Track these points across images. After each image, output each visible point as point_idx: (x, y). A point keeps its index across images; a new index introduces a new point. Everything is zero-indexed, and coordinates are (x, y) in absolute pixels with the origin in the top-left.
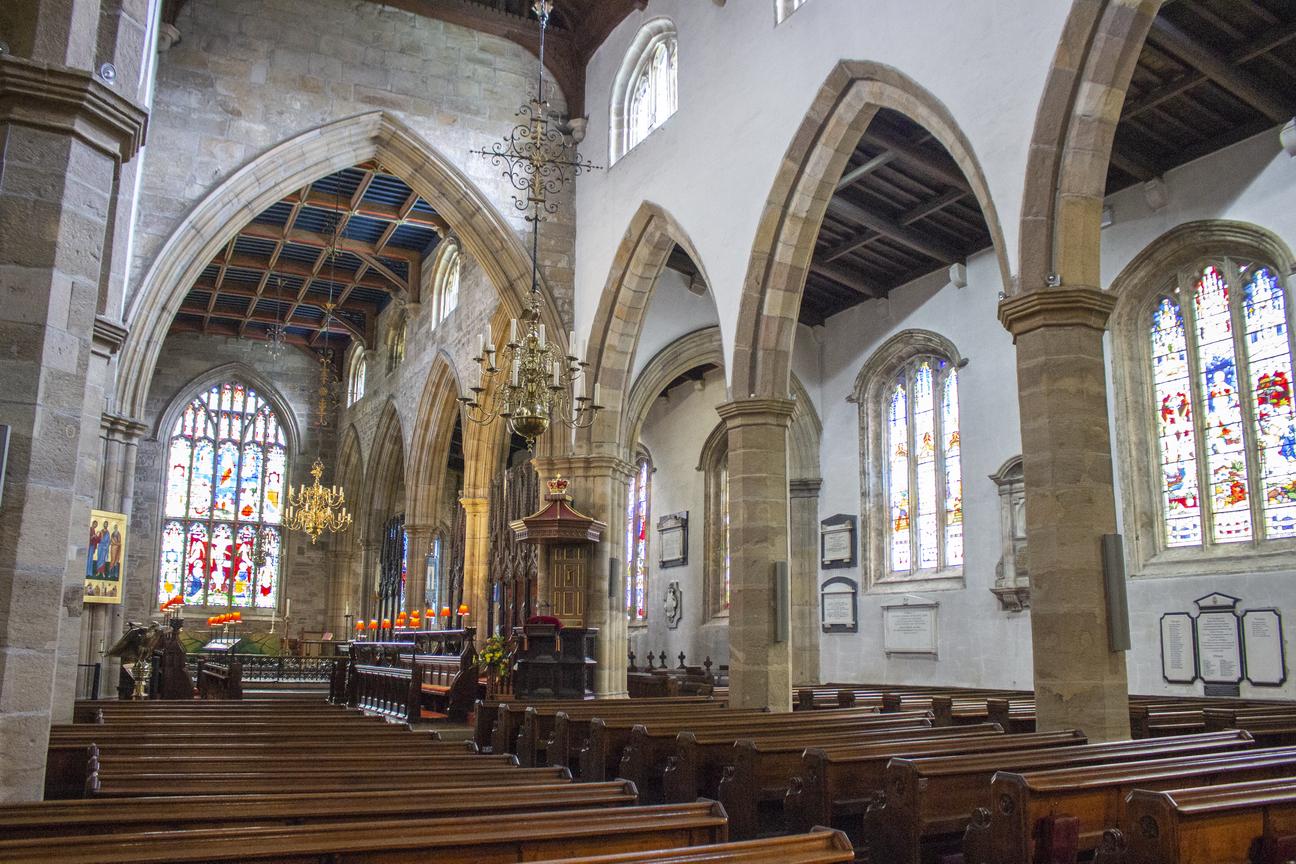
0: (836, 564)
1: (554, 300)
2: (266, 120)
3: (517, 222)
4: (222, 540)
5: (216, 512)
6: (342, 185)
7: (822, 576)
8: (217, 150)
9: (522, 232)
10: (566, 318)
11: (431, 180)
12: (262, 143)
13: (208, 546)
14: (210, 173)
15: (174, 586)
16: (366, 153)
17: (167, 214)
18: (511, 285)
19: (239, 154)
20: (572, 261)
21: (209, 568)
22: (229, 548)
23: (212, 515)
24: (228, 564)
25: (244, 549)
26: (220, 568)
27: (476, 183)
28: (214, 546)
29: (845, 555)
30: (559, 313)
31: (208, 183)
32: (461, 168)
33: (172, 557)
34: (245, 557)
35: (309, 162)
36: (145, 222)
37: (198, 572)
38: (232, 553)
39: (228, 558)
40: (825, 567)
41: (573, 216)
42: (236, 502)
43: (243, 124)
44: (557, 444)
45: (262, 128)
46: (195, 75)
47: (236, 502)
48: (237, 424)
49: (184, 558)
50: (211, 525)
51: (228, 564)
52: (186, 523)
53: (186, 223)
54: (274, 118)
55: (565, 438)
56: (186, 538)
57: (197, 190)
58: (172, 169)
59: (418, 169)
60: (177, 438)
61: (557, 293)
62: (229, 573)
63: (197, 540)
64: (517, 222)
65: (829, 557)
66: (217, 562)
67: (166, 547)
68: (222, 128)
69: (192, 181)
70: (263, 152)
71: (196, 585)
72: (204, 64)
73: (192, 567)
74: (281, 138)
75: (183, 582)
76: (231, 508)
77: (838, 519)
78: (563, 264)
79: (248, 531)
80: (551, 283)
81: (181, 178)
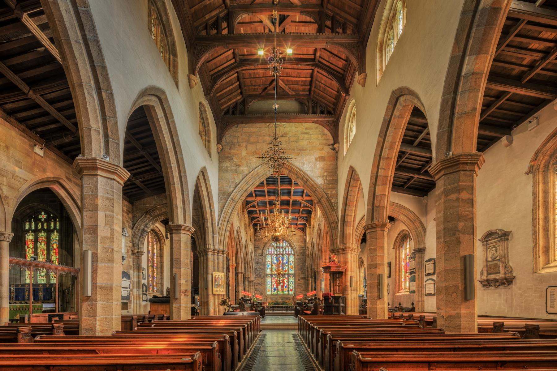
0: (429, 274)
2: (247, 166)
7: (425, 278)
8: (235, 177)
9: (321, 184)
10: (335, 208)
11: (294, 173)
12: (247, 173)
20: (337, 190)
27: (306, 172)
29: (432, 271)
32: (302, 168)
35: (260, 175)
40: (426, 275)
41: (337, 176)
43: (241, 168)
54: (249, 165)
58: (225, 185)
59: (290, 171)
61: (332, 201)
64: (320, 181)
65: (427, 272)
68: (236, 171)
69: (230, 187)
70: (247, 175)
77: (430, 260)
78: (334, 192)
81: (227, 186)
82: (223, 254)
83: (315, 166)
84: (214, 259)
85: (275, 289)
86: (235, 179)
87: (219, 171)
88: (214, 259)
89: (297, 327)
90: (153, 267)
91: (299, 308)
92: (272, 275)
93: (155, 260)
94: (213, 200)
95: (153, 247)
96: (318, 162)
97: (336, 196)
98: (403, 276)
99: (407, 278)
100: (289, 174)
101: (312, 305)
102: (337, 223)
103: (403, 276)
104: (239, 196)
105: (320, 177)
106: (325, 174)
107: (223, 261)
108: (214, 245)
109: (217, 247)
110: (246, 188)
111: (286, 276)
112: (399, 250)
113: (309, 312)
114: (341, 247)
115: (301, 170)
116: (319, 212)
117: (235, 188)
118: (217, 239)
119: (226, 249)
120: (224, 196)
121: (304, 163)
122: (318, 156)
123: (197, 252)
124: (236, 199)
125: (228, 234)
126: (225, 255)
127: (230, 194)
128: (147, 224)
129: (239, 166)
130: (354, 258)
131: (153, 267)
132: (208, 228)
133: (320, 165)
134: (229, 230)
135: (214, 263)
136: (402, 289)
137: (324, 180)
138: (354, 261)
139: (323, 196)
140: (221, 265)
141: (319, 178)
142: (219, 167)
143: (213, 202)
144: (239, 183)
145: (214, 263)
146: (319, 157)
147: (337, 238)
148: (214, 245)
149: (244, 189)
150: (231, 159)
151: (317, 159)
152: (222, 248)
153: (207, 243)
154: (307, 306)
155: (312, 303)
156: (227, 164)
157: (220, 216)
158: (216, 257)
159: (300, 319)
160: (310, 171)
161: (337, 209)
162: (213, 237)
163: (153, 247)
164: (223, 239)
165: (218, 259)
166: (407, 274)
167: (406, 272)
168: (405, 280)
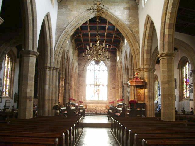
1: (135, 37)
2: (77, 11)
3: (127, 22)
6: (92, 21)
9: (128, 24)
10: (138, 40)
14: (67, 23)
16: (96, 13)
17: (60, 31)
18: (127, 35)
19: (72, 18)
20: (138, 28)
27: (117, 16)
30: (136, 39)
31: (67, 24)
32: (114, 14)
36: (57, 32)
41: (138, 20)
43: (73, 13)
44: (137, 66)
45: (76, 13)
46: (64, 6)
53: (64, 32)
55: (139, 64)
57: (65, 26)
61: (136, 36)
64: (127, 22)
69: (64, 24)
71: (93, 96)
72: (66, 3)
74: (80, 14)
78: (137, 29)
80: (134, 34)
82: (57, 70)
83: (123, 13)
84: (50, 74)
85: (93, 96)
86: (68, 19)
87: (58, 14)
88: (50, 74)
89: (111, 126)
90: (7, 78)
91: (111, 111)
92: (90, 85)
93: (9, 73)
94: (52, 33)
95: (8, 64)
96: (125, 11)
97: (138, 32)
98: (185, 88)
99: (188, 90)
100: (105, 17)
101: (121, 109)
102: (139, 51)
103: (185, 88)
104: (71, 31)
105: (126, 19)
106: (130, 18)
107: (56, 75)
108: (50, 64)
109: (53, 65)
110: (76, 25)
111: (101, 86)
112: (182, 70)
113: (118, 114)
114: (142, 67)
115: (114, 15)
116: (126, 41)
117: (68, 25)
118: (53, 60)
119: (59, 67)
120: (60, 30)
121: (116, 11)
122: (125, 7)
123: (38, 68)
124: (68, 33)
125: (61, 56)
126: (58, 71)
127: (64, 29)
128: (6, 49)
129: (72, 11)
130: (151, 75)
131: (7, 78)
132: (47, 52)
133: (126, 12)
134: (62, 53)
135: (50, 77)
136: (184, 98)
137: (129, 22)
138: (151, 78)
139: (129, 32)
140: (54, 78)
141: (126, 21)
142: (58, 12)
143: (52, 34)
144: (71, 22)
145: (50, 77)
146: (126, 7)
147: (139, 61)
148: (50, 64)
149: (74, 26)
150: (66, 7)
151: (124, 9)
152: (56, 66)
153: (46, 62)
154: (117, 109)
155: (120, 107)
156: (64, 10)
157: (56, 43)
158: (51, 72)
159: (112, 120)
160: (120, 15)
161: (139, 41)
162: (50, 58)
163: (8, 64)
164: (57, 60)
165: (53, 73)
166: (188, 87)
167: (187, 86)
168: (186, 91)
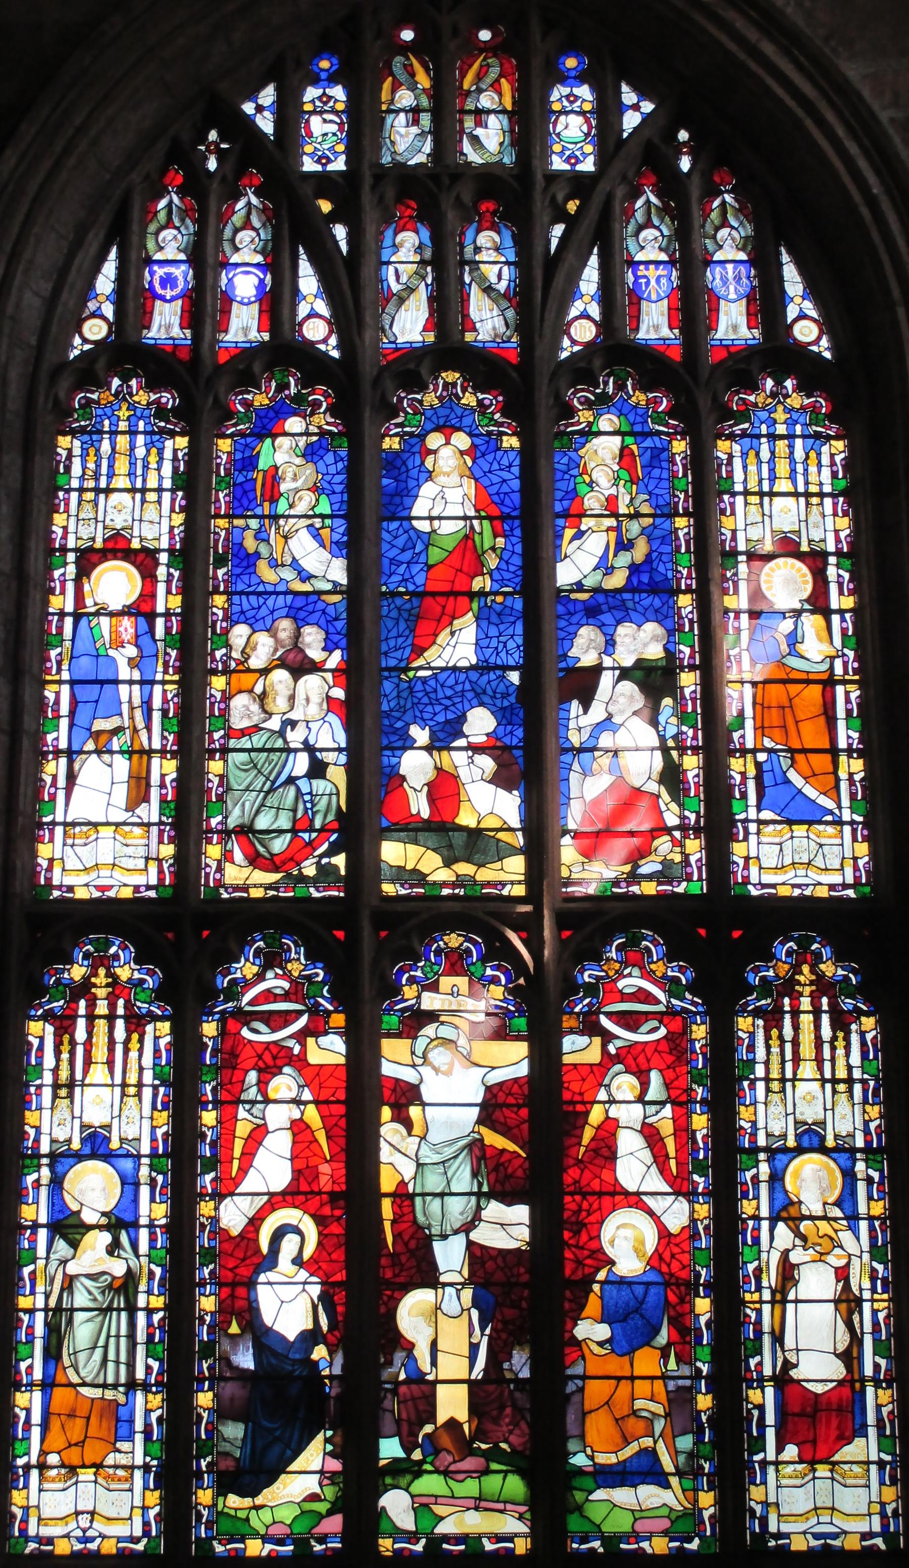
4: (455, 1064)
5: (393, 852)
13: (361, 1102)
15: (117, 1422)
21: (372, 1257)
22: (495, 1106)
23: (365, 868)
24: (508, 1226)
25: (626, 1107)
26: (450, 1256)
28: (406, 1096)
33: (93, 1189)
34: (633, 1167)
37: (288, 1304)
38: (540, 1143)
39: (499, 1180)
42: (530, 765)
47: (530, 765)
48: (491, 255)
49: (183, 1199)
50: (365, 948)
51: (508, 1226)
52: (183, 937)
56: (185, 1044)
60: (90, 371)
62: (527, 1298)
63: (272, 1061)
66: (429, 1212)
67: (49, 1123)
73: (245, 1260)
75: (177, 1385)
76: (491, 805)
79: (641, 980)
